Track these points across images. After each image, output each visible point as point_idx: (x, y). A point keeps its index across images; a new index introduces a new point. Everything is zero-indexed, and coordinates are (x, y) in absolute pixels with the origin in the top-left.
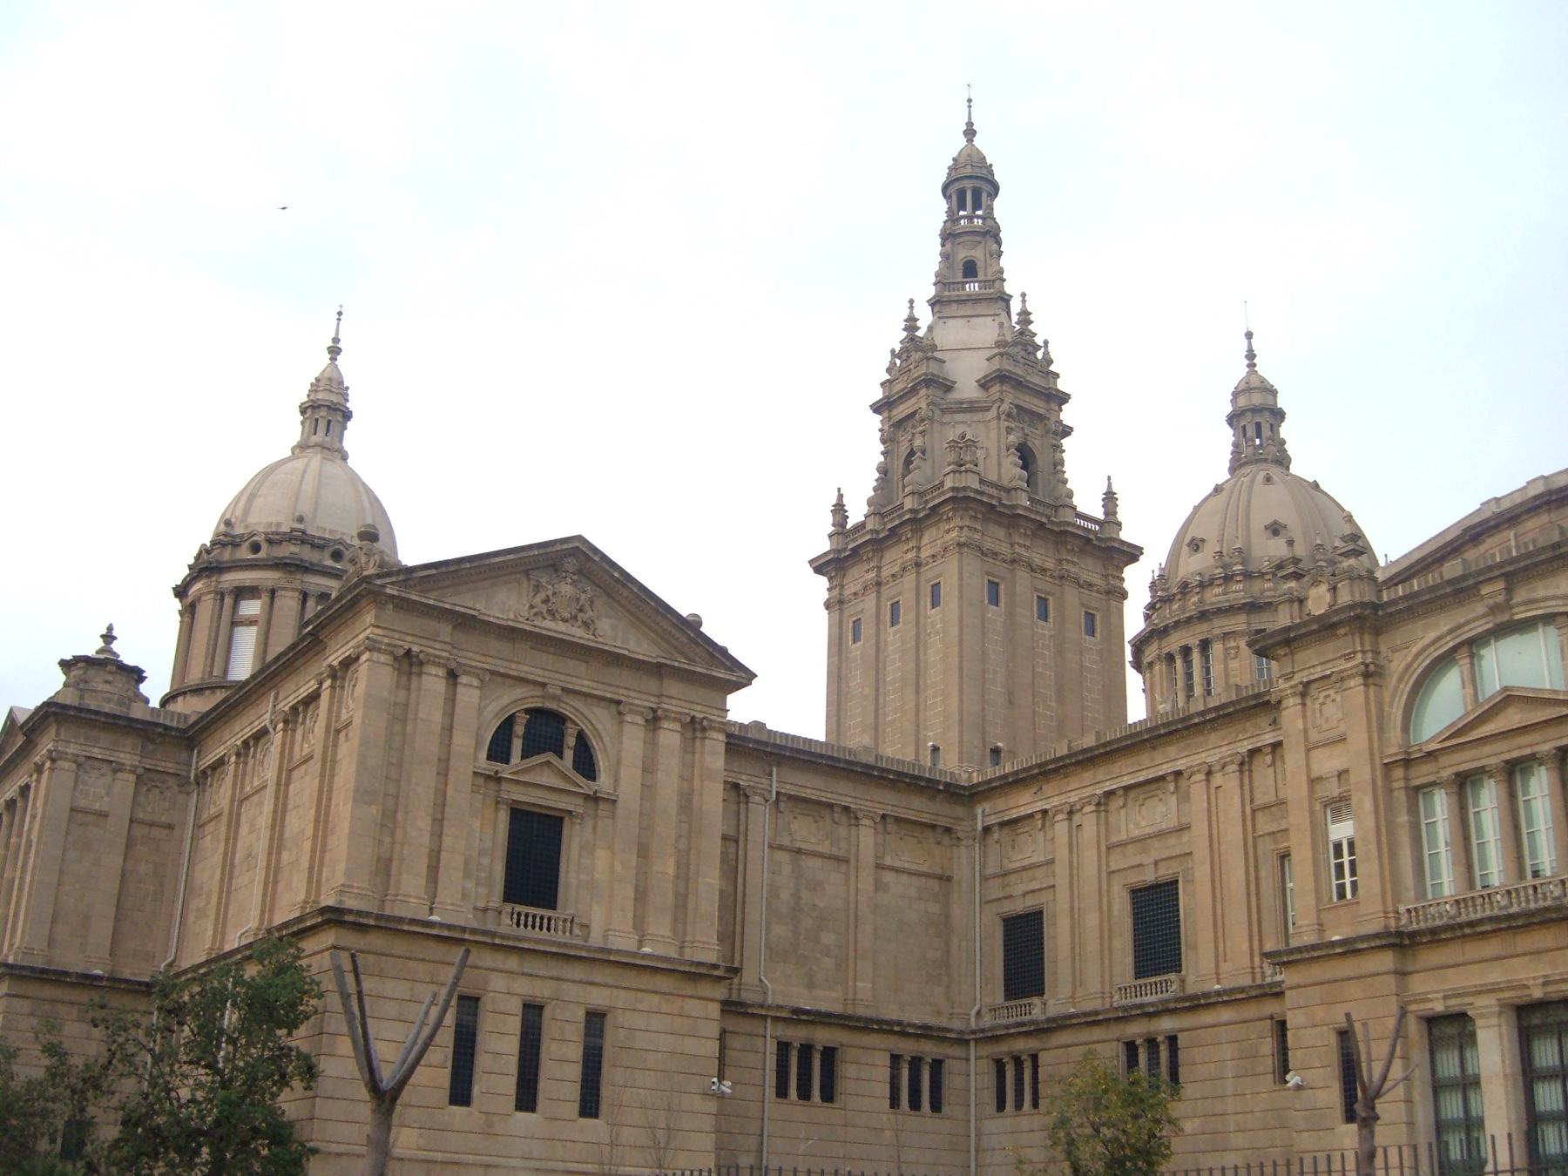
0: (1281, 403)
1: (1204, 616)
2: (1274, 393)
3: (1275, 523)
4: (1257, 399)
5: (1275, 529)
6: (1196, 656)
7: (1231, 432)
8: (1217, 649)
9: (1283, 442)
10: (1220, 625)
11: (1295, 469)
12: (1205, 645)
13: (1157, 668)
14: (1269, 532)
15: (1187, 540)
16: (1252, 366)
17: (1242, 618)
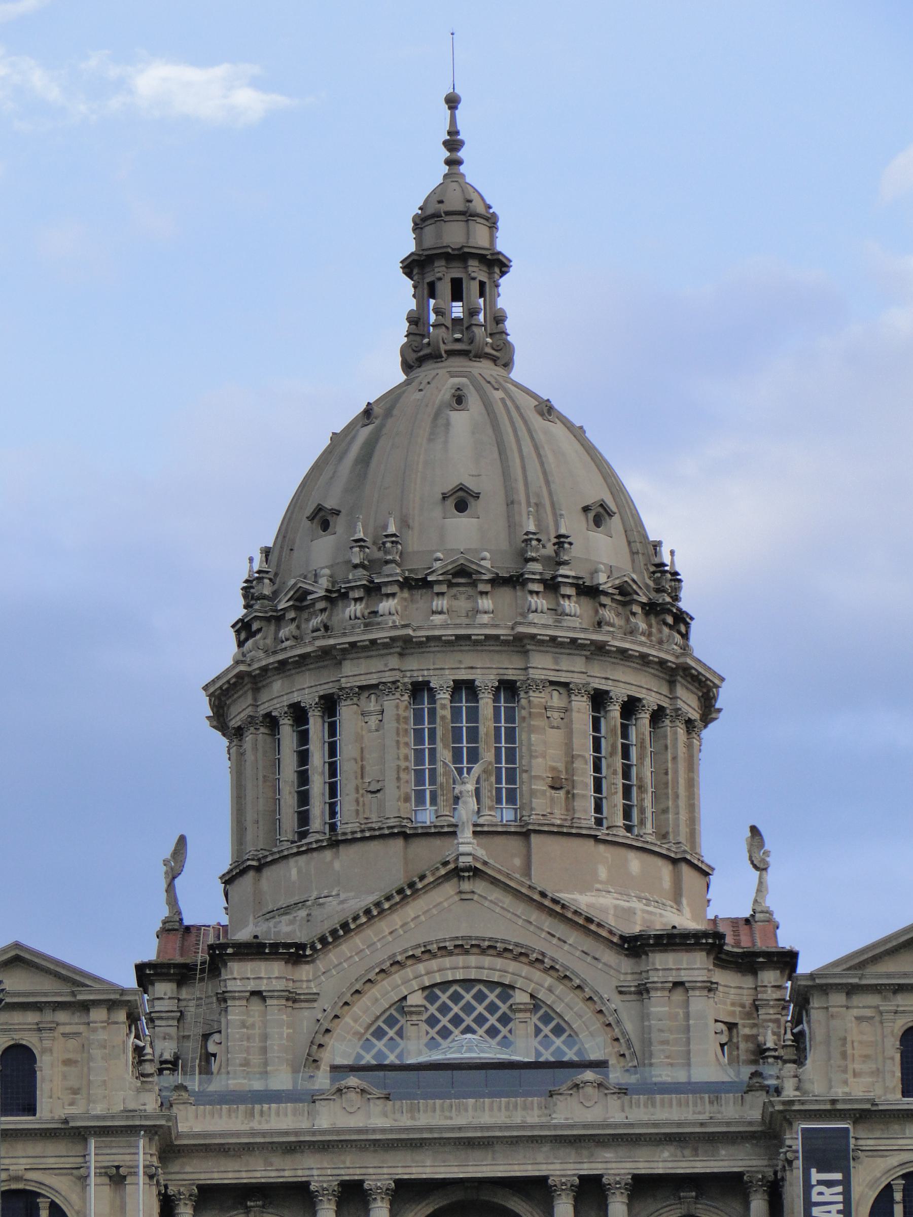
0: (504, 245)
1: (330, 657)
2: (491, 221)
3: (461, 488)
5: (462, 500)
6: (316, 726)
7: (408, 284)
8: (347, 713)
9: (499, 319)
10: (354, 672)
12: (329, 705)
13: (249, 739)
14: (451, 503)
15: (310, 509)
16: (453, 163)
17: (394, 662)
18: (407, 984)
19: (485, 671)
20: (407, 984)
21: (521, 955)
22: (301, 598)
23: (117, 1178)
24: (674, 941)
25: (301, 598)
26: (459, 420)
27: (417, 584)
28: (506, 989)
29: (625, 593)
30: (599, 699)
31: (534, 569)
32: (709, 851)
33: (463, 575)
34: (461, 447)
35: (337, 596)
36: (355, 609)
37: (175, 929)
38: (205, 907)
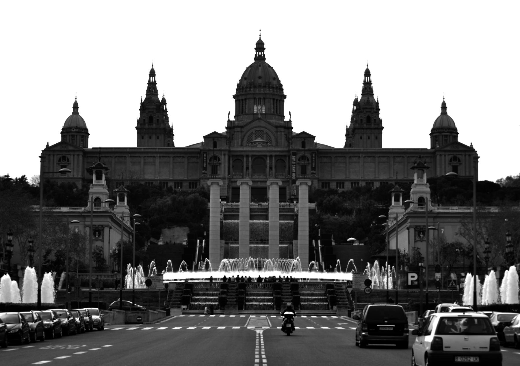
4: (260, 46)
5: (260, 78)
6: (244, 101)
8: (247, 101)
9: (264, 55)
10: (249, 96)
11: (266, 61)
12: (246, 99)
18: (253, 131)
19: (262, 97)
20: (253, 131)
21: (265, 128)
22: (243, 87)
23: (225, 155)
24: (281, 127)
25: (243, 87)
26: (260, 68)
27: (255, 87)
28: (263, 131)
29: (277, 88)
30: (274, 99)
31: (267, 85)
32: (285, 114)
33: (260, 86)
34: (260, 72)
35: (246, 88)
36: (248, 89)
37: (229, 121)
38: (232, 119)
